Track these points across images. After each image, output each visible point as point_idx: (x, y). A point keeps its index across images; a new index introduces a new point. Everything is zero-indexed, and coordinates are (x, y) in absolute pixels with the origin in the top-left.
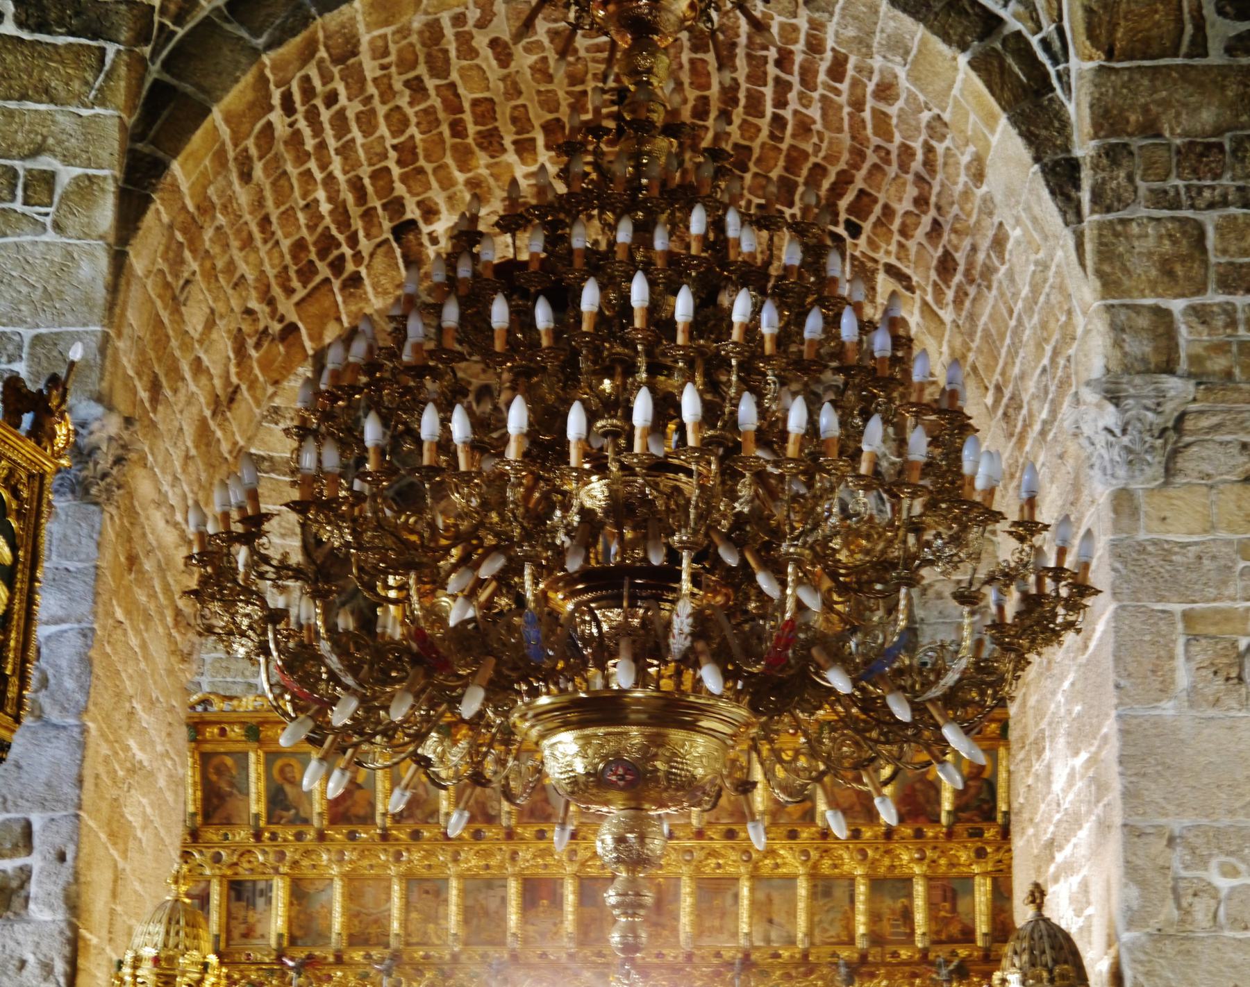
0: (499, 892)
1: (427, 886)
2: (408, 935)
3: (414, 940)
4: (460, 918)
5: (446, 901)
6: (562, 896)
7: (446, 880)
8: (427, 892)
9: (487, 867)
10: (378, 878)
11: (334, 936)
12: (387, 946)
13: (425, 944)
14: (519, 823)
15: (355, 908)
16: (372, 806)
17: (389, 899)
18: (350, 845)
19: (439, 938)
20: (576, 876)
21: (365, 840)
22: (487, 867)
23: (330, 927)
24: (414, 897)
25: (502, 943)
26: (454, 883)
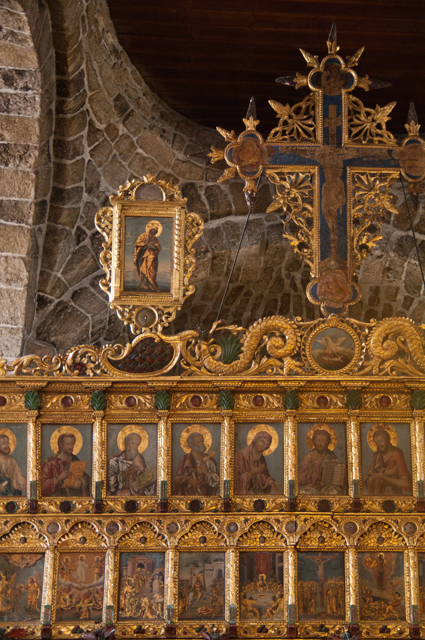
0: (216, 566)
1: (140, 559)
2: (119, 609)
3: (128, 614)
4: (175, 591)
5: (162, 575)
6: (281, 569)
7: (163, 553)
8: (141, 566)
9: (204, 540)
10: (91, 552)
11: (43, 610)
12: (99, 620)
13: (138, 619)
14: (237, 492)
15: (65, 581)
16: (88, 477)
17: (101, 573)
18: (64, 517)
19: (153, 612)
20: (297, 550)
21: (79, 511)
22: (204, 540)
23: (39, 602)
24: (128, 572)
25: (220, 616)
26: (170, 555)
